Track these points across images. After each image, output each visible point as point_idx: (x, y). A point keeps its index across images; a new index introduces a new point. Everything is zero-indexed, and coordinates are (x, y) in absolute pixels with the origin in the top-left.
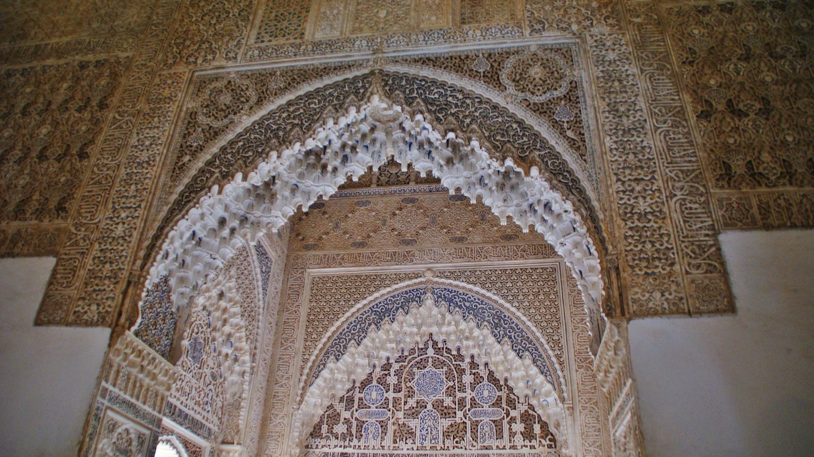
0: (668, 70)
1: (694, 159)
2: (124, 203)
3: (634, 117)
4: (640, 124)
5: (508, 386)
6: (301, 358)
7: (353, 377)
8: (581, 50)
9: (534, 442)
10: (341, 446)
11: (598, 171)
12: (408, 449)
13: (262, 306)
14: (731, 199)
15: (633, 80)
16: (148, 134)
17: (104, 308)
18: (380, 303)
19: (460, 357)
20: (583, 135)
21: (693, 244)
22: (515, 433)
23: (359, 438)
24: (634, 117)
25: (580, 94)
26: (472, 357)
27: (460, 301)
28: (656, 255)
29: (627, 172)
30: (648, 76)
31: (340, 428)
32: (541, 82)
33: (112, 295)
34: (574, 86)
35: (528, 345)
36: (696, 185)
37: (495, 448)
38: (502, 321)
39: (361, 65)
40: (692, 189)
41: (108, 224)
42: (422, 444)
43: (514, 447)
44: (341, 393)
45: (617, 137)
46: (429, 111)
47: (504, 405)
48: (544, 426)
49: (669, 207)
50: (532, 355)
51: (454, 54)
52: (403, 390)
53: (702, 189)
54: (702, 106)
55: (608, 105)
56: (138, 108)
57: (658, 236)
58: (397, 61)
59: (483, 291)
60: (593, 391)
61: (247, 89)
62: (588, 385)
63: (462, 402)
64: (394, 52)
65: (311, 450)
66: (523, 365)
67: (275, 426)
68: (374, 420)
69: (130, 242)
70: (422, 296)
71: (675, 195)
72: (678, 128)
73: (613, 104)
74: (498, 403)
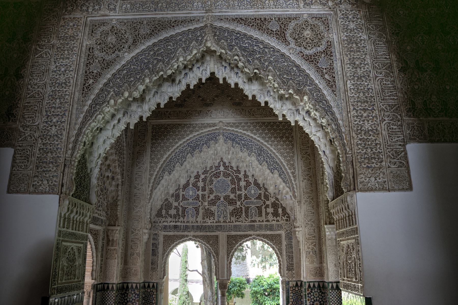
0: (384, 38)
1: (395, 98)
2: (53, 112)
3: (364, 69)
4: (367, 73)
5: (264, 188)
6: (148, 173)
9: (278, 218)
10: (173, 222)
11: (342, 102)
12: (211, 223)
13: (125, 145)
14: (414, 124)
15: (364, 43)
16: (62, 62)
17: (52, 183)
18: (193, 141)
19: (238, 171)
20: (334, 77)
21: (392, 151)
22: (269, 213)
23: (184, 216)
24: (364, 69)
25: (333, 50)
26: (245, 171)
27: (239, 141)
28: (373, 156)
29: (359, 104)
30: (372, 41)
31: (173, 212)
32: (311, 41)
33: (55, 174)
34: (330, 44)
35: (276, 166)
36: (396, 114)
37: (258, 221)
38: (262, 152)
39: (198, 20)
40: (394, 117)
42: (218, 219)
43: (268, 221)
44: (171, 192)
45: (354, 82)
46: (243, 56)
47: (263, 198)
48: (284, 209)
49: (381, 127)
50: (279, 172)
52: (207, 190)
53: (399, 117)
54: (402, 63)
55: (350, 59)
56: (52, 43)
57: (374, 145)
58: (221, 19)
59: (252, 135)
60: (311, 192)
61: (125, 33)
62: (308, 189)
63: (240, 196)
65: (157, 224)
67: (137, 212)
68: (191, 207)
69: (62, 139)
70: (217, 137)
71: (385, 120)
72: (388, 77)
73: (352, 59)
74: (259, 197)
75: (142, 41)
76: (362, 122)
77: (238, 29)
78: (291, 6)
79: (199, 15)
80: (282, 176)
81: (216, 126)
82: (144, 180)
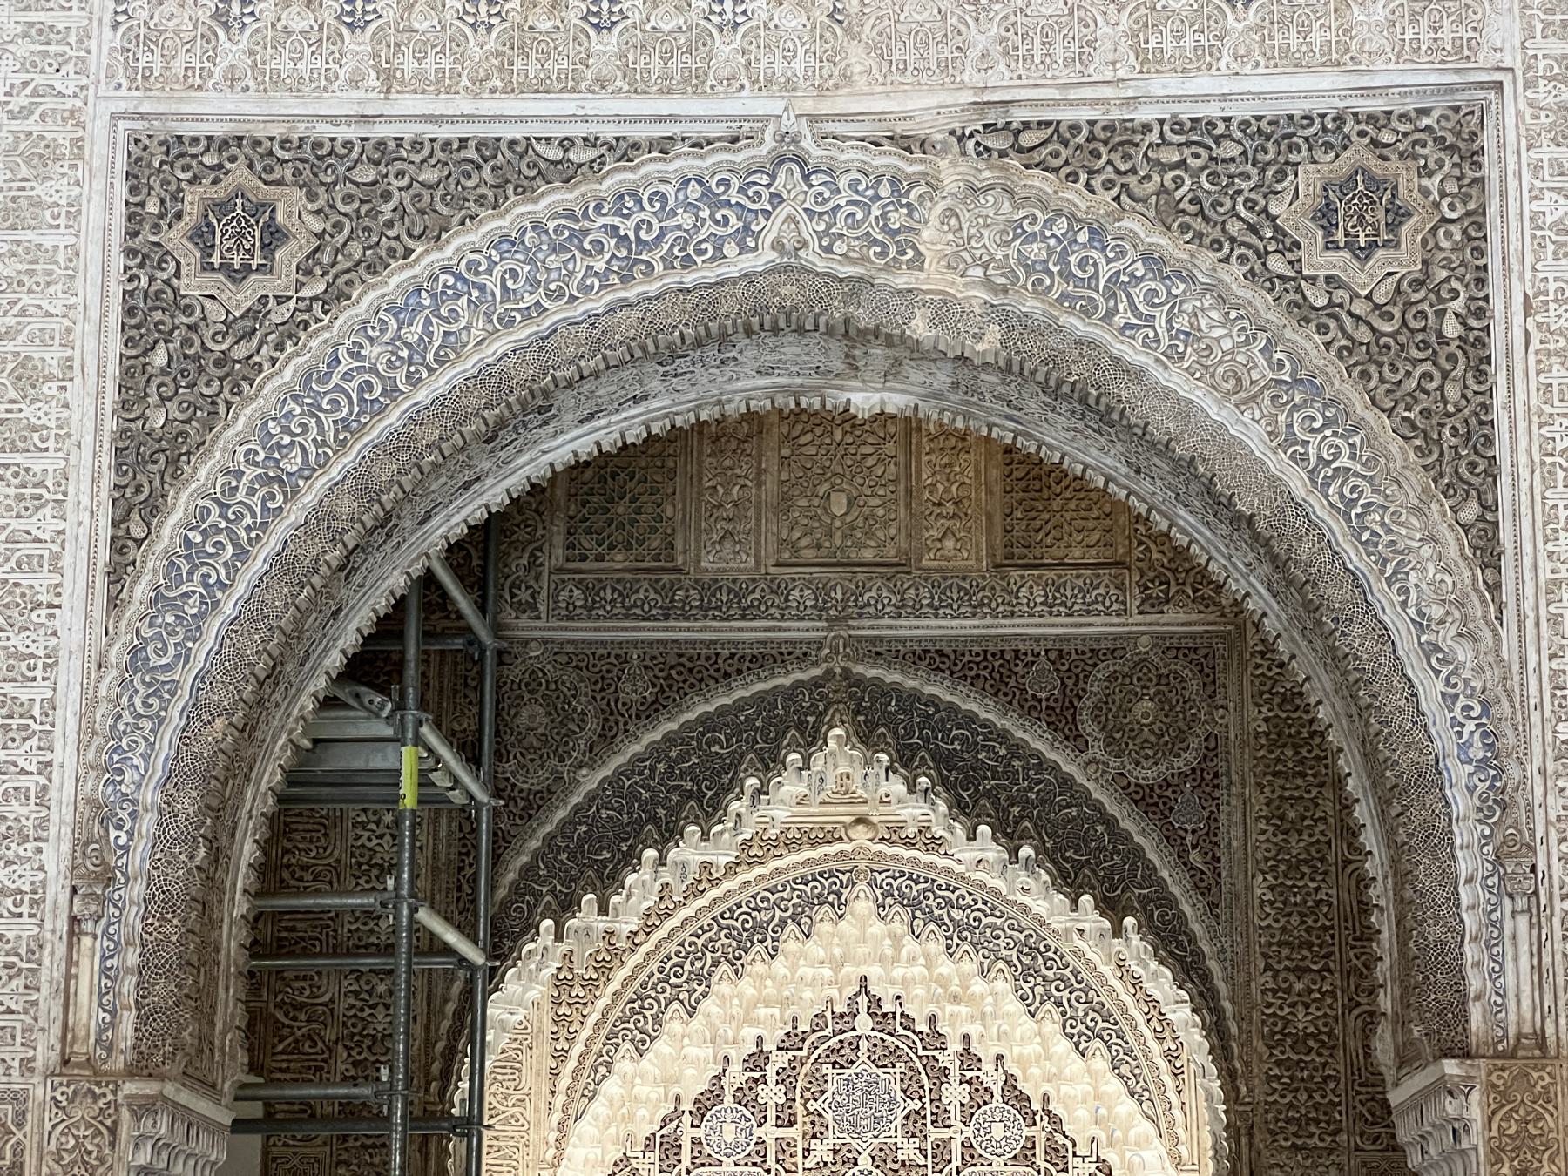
6: (547, 1049)
7: (676, 1089)
8: (1235, 656)
18: (739, 906)
19: (936, 1038)
20: (1219, 860)
21: (1372, 1099)
24: (1311, 836)
25: (1222, 767)
26: (966, 1038)
28: (1313, 1115)
29: (1285, 952)
32: (1153, 739)
34: (1213, 748)
39: (805, 654)
41: (352, 1007)
45: (1276, 878)
46: (944, 782)
47: (1040, 1160)
49: (1345, 1026)
50: (1109, 1048)
51: (991, 649)
58: (878, 654)
63: (942, 1146)
64: (871, 627)
66: (1088, 1071)
70: (845, 892)
71: (1358, 1004)
73: (1277, 803)
75: (632, 728)
76: (1287, 1010)
77: (930, 690)
78: (1100, 608)
79: (807, 634)
80: (1123, 1069)
81: (841, 838)
82: (527, 1080)
